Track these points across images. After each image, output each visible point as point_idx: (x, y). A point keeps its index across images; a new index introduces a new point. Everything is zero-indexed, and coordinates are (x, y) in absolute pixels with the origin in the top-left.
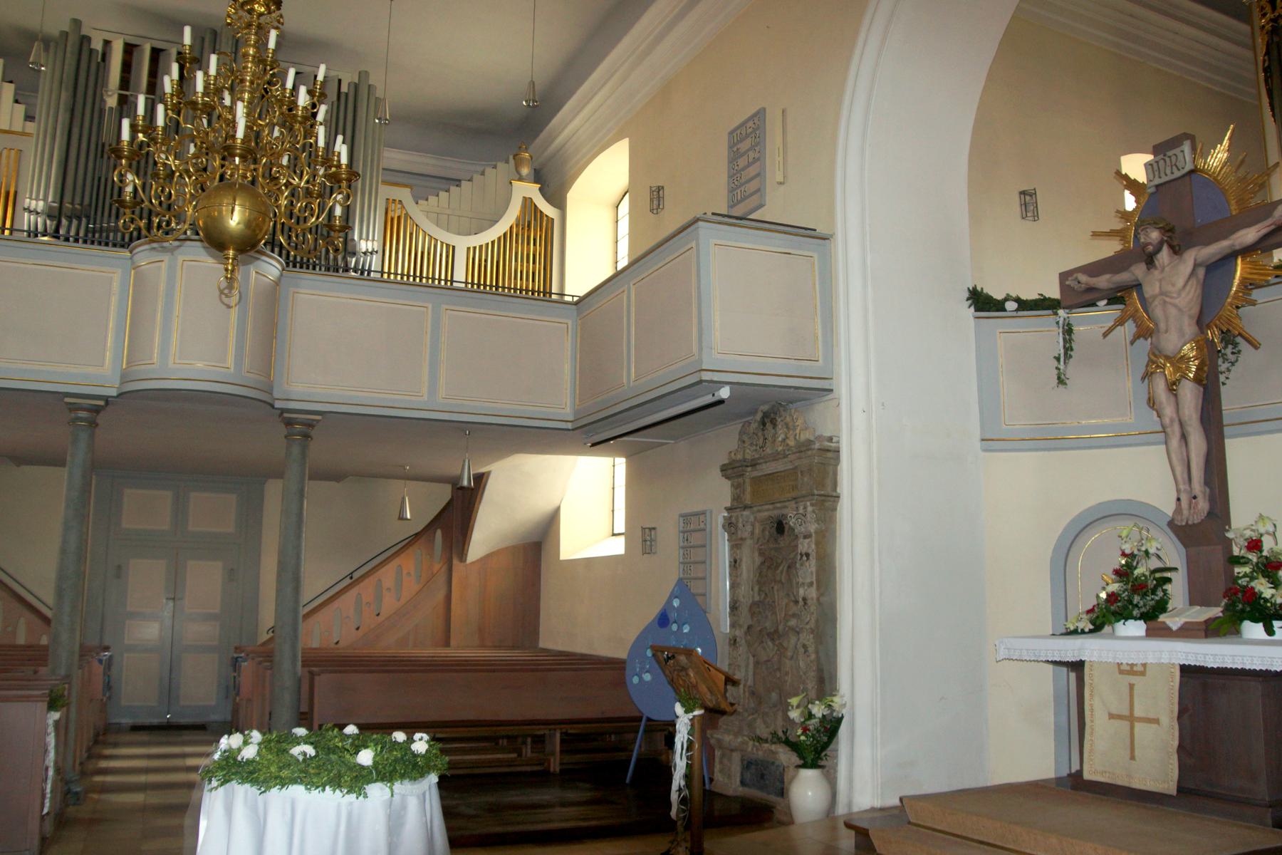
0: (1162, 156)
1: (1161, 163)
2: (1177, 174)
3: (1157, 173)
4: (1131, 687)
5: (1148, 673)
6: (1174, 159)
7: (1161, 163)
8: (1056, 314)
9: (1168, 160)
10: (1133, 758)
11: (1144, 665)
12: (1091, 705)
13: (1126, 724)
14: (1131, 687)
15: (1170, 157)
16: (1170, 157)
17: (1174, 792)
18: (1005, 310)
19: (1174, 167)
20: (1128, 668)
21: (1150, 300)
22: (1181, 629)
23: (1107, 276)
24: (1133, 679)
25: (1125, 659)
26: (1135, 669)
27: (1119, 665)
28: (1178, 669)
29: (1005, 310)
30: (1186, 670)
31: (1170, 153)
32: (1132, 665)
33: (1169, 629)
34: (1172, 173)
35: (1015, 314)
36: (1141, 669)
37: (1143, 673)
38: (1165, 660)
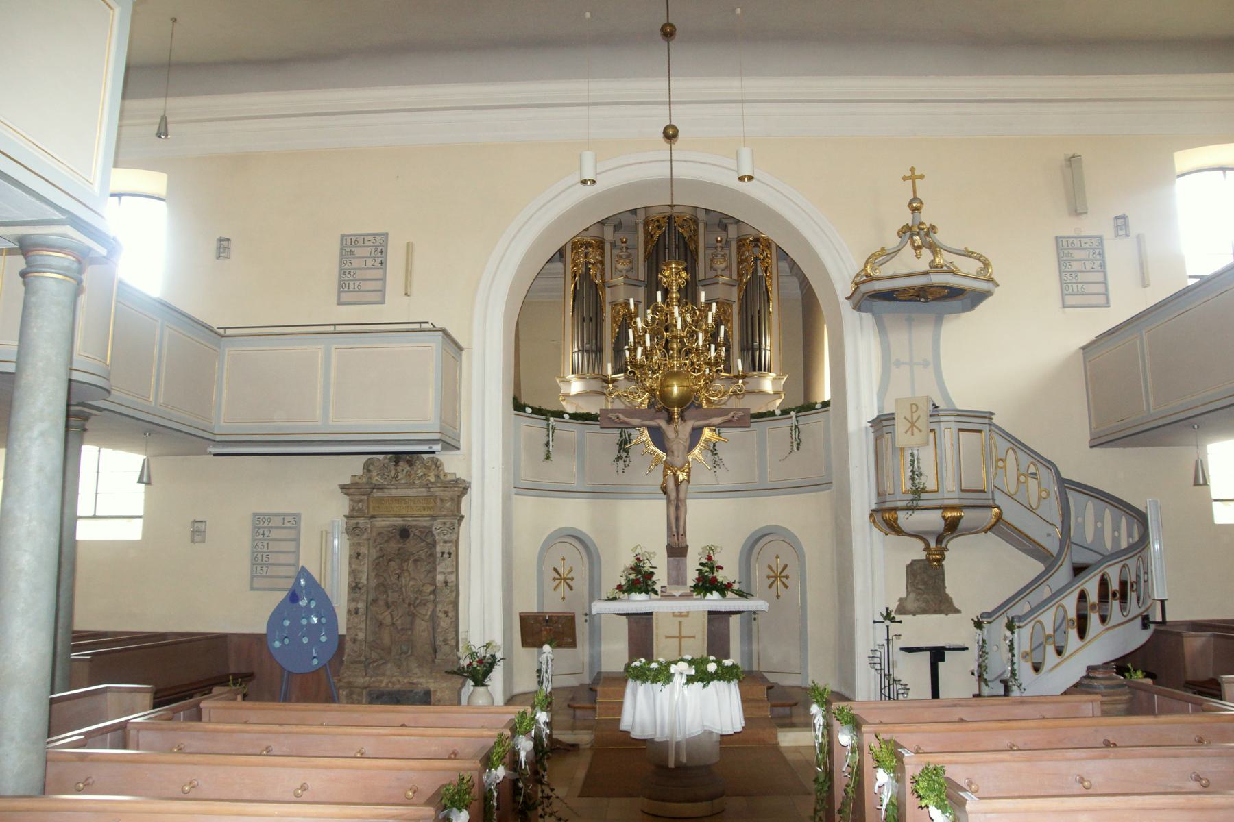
4: (680, 622)
5: (690, 616)
8: (548, 420)
11: (688, 612)
12: (657, 633)
14: (680, 622)
18: (525, 412)
20: (678, 614)
22: (680, 596)
23: (639, 420)
24: (680, 619)
26: (683, 614)
27: (673, 613)
28: (707, 612)
29: (525, 412)
30: (710, 613)
33: (674, 596)
35: (530, 415)
36: (686, 614)
37: (687, 616)
38: (701, 609)
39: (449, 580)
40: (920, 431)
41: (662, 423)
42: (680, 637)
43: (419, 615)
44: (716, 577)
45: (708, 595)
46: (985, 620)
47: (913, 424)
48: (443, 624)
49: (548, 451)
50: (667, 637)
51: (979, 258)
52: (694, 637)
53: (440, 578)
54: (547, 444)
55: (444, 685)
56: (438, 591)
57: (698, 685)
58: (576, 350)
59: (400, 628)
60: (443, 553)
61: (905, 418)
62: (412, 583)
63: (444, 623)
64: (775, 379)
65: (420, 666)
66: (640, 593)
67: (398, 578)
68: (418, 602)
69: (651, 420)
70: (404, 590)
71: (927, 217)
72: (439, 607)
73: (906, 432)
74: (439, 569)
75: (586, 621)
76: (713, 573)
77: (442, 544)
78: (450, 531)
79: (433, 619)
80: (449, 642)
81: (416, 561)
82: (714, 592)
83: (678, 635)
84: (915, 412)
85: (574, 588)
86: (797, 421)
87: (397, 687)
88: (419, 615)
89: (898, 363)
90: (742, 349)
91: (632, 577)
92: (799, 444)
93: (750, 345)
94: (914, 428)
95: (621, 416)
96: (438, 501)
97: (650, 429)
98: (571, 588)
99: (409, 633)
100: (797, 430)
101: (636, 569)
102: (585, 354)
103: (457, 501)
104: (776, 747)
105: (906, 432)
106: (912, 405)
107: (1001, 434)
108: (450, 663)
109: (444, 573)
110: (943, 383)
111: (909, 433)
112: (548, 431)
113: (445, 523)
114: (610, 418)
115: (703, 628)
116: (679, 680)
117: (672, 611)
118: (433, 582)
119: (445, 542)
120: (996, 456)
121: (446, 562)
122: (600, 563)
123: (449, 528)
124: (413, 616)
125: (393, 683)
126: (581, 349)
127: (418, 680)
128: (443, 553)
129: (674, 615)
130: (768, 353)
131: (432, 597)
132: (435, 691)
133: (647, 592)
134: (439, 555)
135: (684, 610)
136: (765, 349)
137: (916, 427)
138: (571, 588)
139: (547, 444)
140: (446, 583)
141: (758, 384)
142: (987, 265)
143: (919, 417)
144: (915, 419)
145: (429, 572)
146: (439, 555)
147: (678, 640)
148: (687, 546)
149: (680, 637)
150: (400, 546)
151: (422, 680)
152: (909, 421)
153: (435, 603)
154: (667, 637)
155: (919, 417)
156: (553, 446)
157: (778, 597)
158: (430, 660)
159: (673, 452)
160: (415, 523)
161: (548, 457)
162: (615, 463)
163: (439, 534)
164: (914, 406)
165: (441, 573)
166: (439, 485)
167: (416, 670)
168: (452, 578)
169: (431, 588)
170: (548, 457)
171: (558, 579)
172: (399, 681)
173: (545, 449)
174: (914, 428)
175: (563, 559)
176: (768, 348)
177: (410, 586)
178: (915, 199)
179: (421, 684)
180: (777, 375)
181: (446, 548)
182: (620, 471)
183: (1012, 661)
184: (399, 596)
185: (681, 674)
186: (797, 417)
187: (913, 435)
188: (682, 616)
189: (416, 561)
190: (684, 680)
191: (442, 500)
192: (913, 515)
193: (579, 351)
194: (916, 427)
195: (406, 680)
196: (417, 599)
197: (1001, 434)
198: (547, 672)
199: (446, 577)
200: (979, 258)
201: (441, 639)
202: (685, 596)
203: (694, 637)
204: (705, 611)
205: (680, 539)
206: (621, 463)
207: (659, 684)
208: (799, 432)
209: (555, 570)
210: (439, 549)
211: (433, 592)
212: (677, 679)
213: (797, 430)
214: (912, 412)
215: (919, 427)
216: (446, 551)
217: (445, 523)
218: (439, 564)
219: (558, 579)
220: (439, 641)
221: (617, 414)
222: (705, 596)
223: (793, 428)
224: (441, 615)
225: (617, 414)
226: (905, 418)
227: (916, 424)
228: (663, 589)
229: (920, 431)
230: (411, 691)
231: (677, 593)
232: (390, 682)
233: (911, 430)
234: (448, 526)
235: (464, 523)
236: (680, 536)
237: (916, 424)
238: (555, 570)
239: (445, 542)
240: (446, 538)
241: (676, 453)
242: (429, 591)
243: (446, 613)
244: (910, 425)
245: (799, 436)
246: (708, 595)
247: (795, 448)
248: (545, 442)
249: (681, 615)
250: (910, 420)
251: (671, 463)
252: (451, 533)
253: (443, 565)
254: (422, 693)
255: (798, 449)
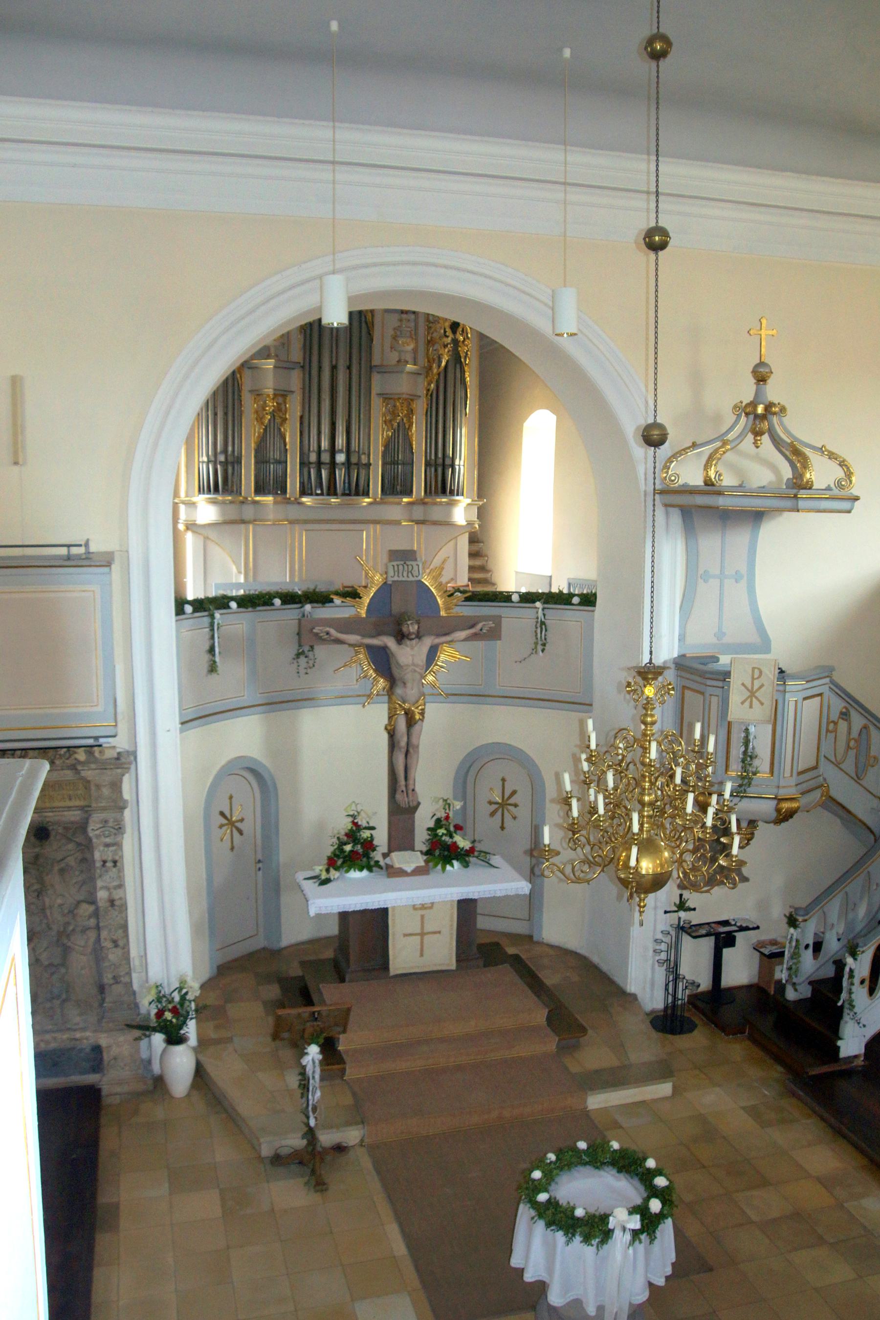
0: (402, 563)
1: (401, 567)
2: (411, 579)
3: (396, 573)
4: (422, 917)
6: (410, 568)
7: (401, 567)
8: (212, 616)
9: (406, 567)
10: (422, 955)
11: (433, 904)
13: (426, 938)
14: (422, 917)
15: (408, 565)
16: (408, 565)
17: (453, 966)
19: (410, 575)
20: (420, 906)
21: (405, 668)
25: (418, 902)
26: (426, 906)
27: (414, 906)
28: (456, 902)
31: (408, 563)
32: (423, 905)
34: (408, 576)
38: (449, 898)
39: (116, 897)
40: (762, 704)
41: (390, 642)
42: (422, 934)
43: (77, 947)
44: (455, 843)
45: (448, 867)
46: (800, 919)
47: (752, 694)
48: (111, 957)
49: (215, 662)
50: (405, 935)
51: (842, 464)
52: (439, 932)
53: (102, 895)
54: (212, 650)
55: (121, 1039)
56: (101, 913)
57: (643, 1237)
58: (205, 459)
59: (46, 963)
60: (105, 862)
61: (743, 684)
62: (59, 901)
63: (113, 956)
64: (469, 504)
65: (81, 1014)
66: (361, 870)
67: (38, 896)
68: (71, 928)
69: (372, 637)
70: (48, 912)
71: (773, 392)
72: (104, 934)
73: (742, 703)
74: (99, 883)
75: (259, 869)
76: (451, 837)
77: (102, 848)
78: (115, 831)
79: (98, 953)
80: (122, 979)
81: (62, 871)
82: (455, 863)
83: (419, 931)
84: (758, 678)
85: (245, 832)
86: (544, 615)
87: (53, 1045)
88: (77, 947)
89: (706, 576)
90: (428, 464)
91: (348, 848)
92: (544, 645)
93: (440, 461)
94: (754, 699)
95: (333, 632)
96: (93, 788)
97: (370, 648)
98: (241, 832)
99: (63, 970)
100: (543, 627)
101: (352, 835)
102: (219, 466)
103: (116, 786)
104: (586, 1114)
105: (742, 703)
106: (753, 669)
107: (839, 692)
108: (125, 1006)
109: (107, 888)
110: (756, 601)
111: (747, 704)
112: (212, 630)
113: (106, 822)
114: (317, 634)
115: (452, 921)
116: (620, 1239)
117: (413, 904)
118: (93, 902)
119: (107, 845)
120: (828, 718)
121: (110, 873)
122: (277, 795)
123: (112, 828)
124: (66, 951)
125: (47, 1042)
126: (212, 458)
127: (83, 1034)
128: (105, 862)
129: (414, 908)
130: (462, 468)
131: (92, 922)
132: (109, 1047)
133: (370, 869)
134: (98, 864)
135: (427, 901)
136: (459, 465)
137: (756, 698)
138: (241, 832)
139: (212, 650)
140: (112, 902)
141: (449, 514)
142: (849, 475)
143: (762, 686)
144: (756, 687)
145: (84, 883)
146: (98, 864)
147: (419, 937)
148: (419, 804)
149: (422, 934)
150: (37, 850)
151: (88, 1034)
152: (748, 690)
153: (98, 928)
154: (405, 935)
155: (762, 686)
156: (220, 653)
157: (502, 828)
158: (96, 1005)
159: (405, 683)
160: (57, 818)
161: (212, 668)
162: (295, 661)
163: (98, 836)
164: (756, 671)
165: (102, 888)
166: (93, 766)
167: (77, 1019)
168: (117, 894)
169: (91, 908)
170: (212, 668)
171: (226, 824)
172: (55, 1039)
173: (206, 657)
174: (754, 699)
175: (231, 797)
176: (462, 463)
177: (56, 906)
178: (761, 364)
179: (87, 1039)
180: (473, 501)
181: (109, 854)
182: (302, 671)
183: (851, 989)
184: (41, 920)
185: (624, 1229)
186: (543, 609)
187: (751, 707)
188: (426, 908)
189: (62, 871)
190: (628, 1237)
191: (98, 787)
192: (740, 804)
193: (209, 462)
194: (756, 698)
195: (65, 1036)
196: (68, 923)
197: (839, 692)
198: (314, 1078)
199: (110, 894)
200: (842, 464)
201: (110, 976)
202: (417, 871)
203: (439, 932)
204: (453, 901)
205: (410, 796)
206: (303, 660)
207: (595, 1242)
208: (546, 631)
209: (222, 814)
210: (97, 855)
211: (96, 914)
212: (618, 1233)
213: (543, 627)
214: (753, 679)
215: (761, 699)
216: (110, 859)
217: (106, 822)
218: (100, 876)
219: (226, 824)
220: (108, 978)
221: (328, 629)
222: (444, 869)
223: (539, 625)
224: (108, 944)
225: (328, 629)
226: (743, 684)
227: (757, 694)
228: (388, 860)
229: (762, 704)
230: (73, 1049)
231: (409, 868)
232: (42, 1041)
233: (749, 700)
234: (111, 824)
235: (127, 813)
236: (410, 792)
237: (757, 694)
238: (222, 814)
239: (107, 845)
240: (108, 840)
241: (409, 685)
242: (87, 914)
243: (115, 943)
244: (749, 694)
245: (545, 635)
246: (448, 867)
247: (540, 648)
248: (207, 647)
249: (423, 907)
250: (750, 688)
251: (402, 698)
252: (115, 834)
253: (107, 877)
254: (88, 1050)
255: (543, 651)
